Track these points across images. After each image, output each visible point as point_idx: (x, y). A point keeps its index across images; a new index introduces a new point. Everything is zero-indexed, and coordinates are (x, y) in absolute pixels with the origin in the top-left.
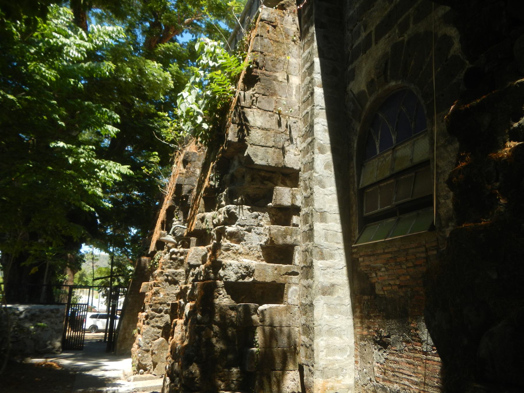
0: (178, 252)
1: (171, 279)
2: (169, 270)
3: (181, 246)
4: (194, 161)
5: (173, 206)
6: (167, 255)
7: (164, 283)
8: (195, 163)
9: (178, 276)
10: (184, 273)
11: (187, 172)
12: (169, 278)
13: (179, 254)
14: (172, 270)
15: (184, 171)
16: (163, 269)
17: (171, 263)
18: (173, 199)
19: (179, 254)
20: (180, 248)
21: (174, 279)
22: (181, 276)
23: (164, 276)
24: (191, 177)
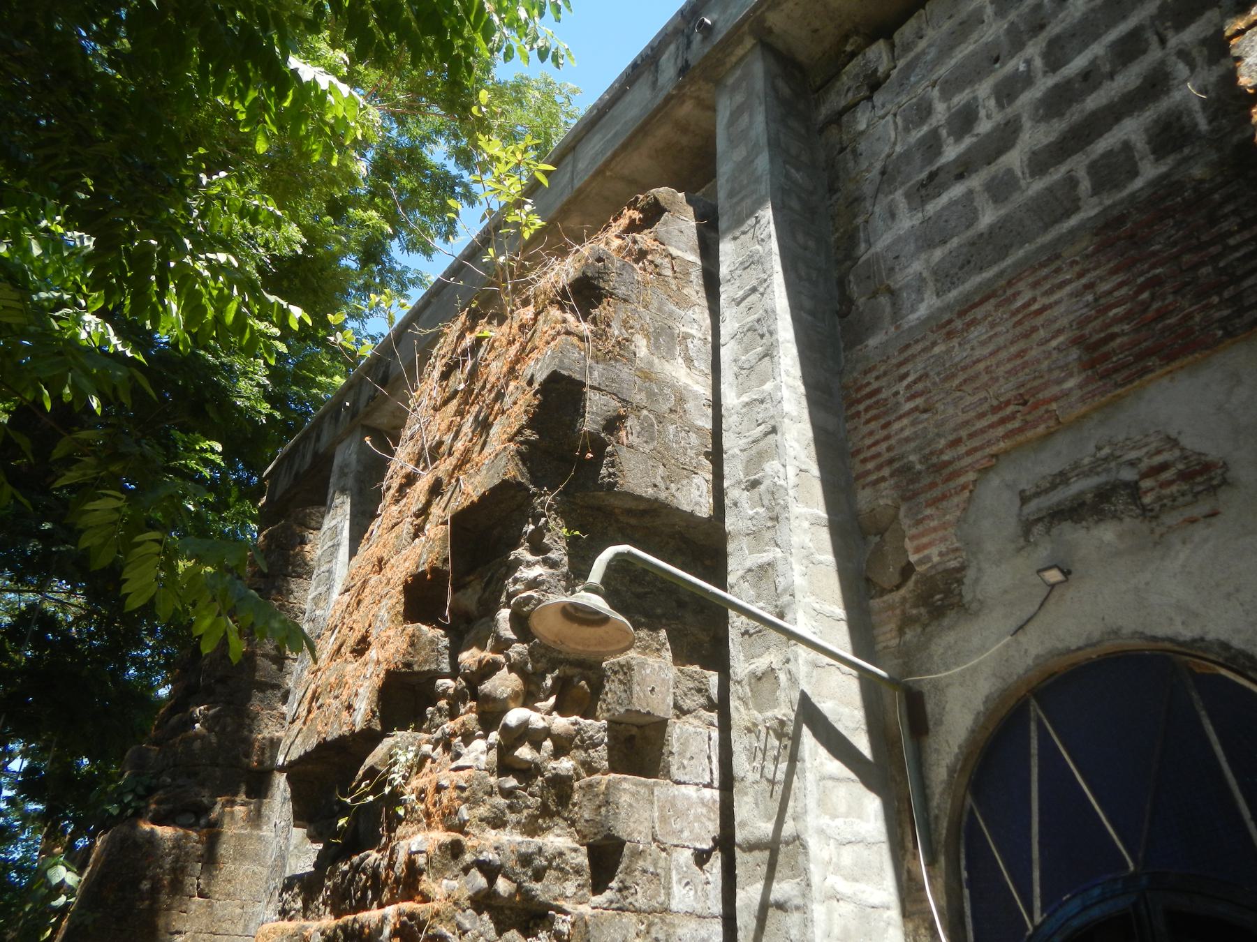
0: (547, 733)
1: (511, 896)
2: (492, 836)
3: (552, 700)
4: (625, 301)
5: (520, 484)
6: (479, 745)
7: (467, 919)
8: (629, 307)
9: (551, 874)
10: (582, 859)
11: (600, 335)
12: (503, 886)
13: (548, 744)
14: (511, 838)
15: (585, 328)
16: (461, 828)
17: (508, 793)
18: (518, 452)
19: (548, 744)
20: (549, 713)
21: (527, 895)
22: (564, 874)
23: (466, 870)
24: (616, 361)
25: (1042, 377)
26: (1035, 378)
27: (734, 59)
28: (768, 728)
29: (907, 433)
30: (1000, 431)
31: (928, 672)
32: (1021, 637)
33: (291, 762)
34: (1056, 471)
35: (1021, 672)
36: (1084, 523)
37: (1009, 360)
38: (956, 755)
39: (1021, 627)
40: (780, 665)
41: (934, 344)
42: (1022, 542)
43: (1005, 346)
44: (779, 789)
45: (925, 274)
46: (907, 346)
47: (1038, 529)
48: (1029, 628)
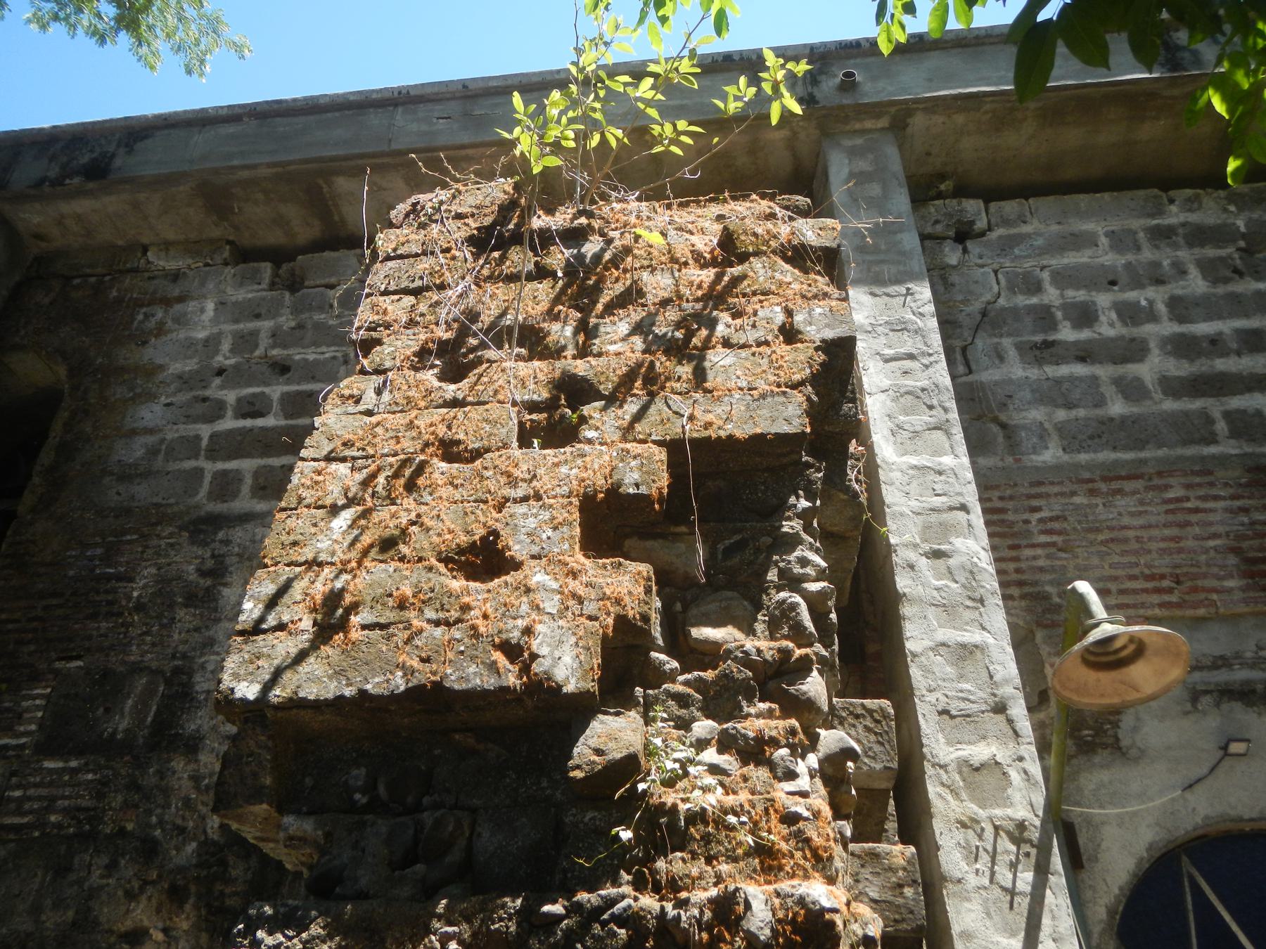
25: (1199, 567)
26: (1192, 565)
27: (858, 126)
28: (996, 828)
29: (1041, 563)
30: (1155, 599)
31: (1078, 804)
32: (1188, 795)
33: (296, 704)
34: (1217, 654)
35: (1190, 828)
36: (1255, 708)
37: (1164, 539)
38: (1116, 897)
39: (1190, 786)
40: (1009, 761)
41: (1073, 494)
42: (1189, 706)
43: (1157, 526)
44: (1023, 903)
45: (1047, 425)
46: (1040, 484)
47: (1206, 701)
48: (1199, 789)
